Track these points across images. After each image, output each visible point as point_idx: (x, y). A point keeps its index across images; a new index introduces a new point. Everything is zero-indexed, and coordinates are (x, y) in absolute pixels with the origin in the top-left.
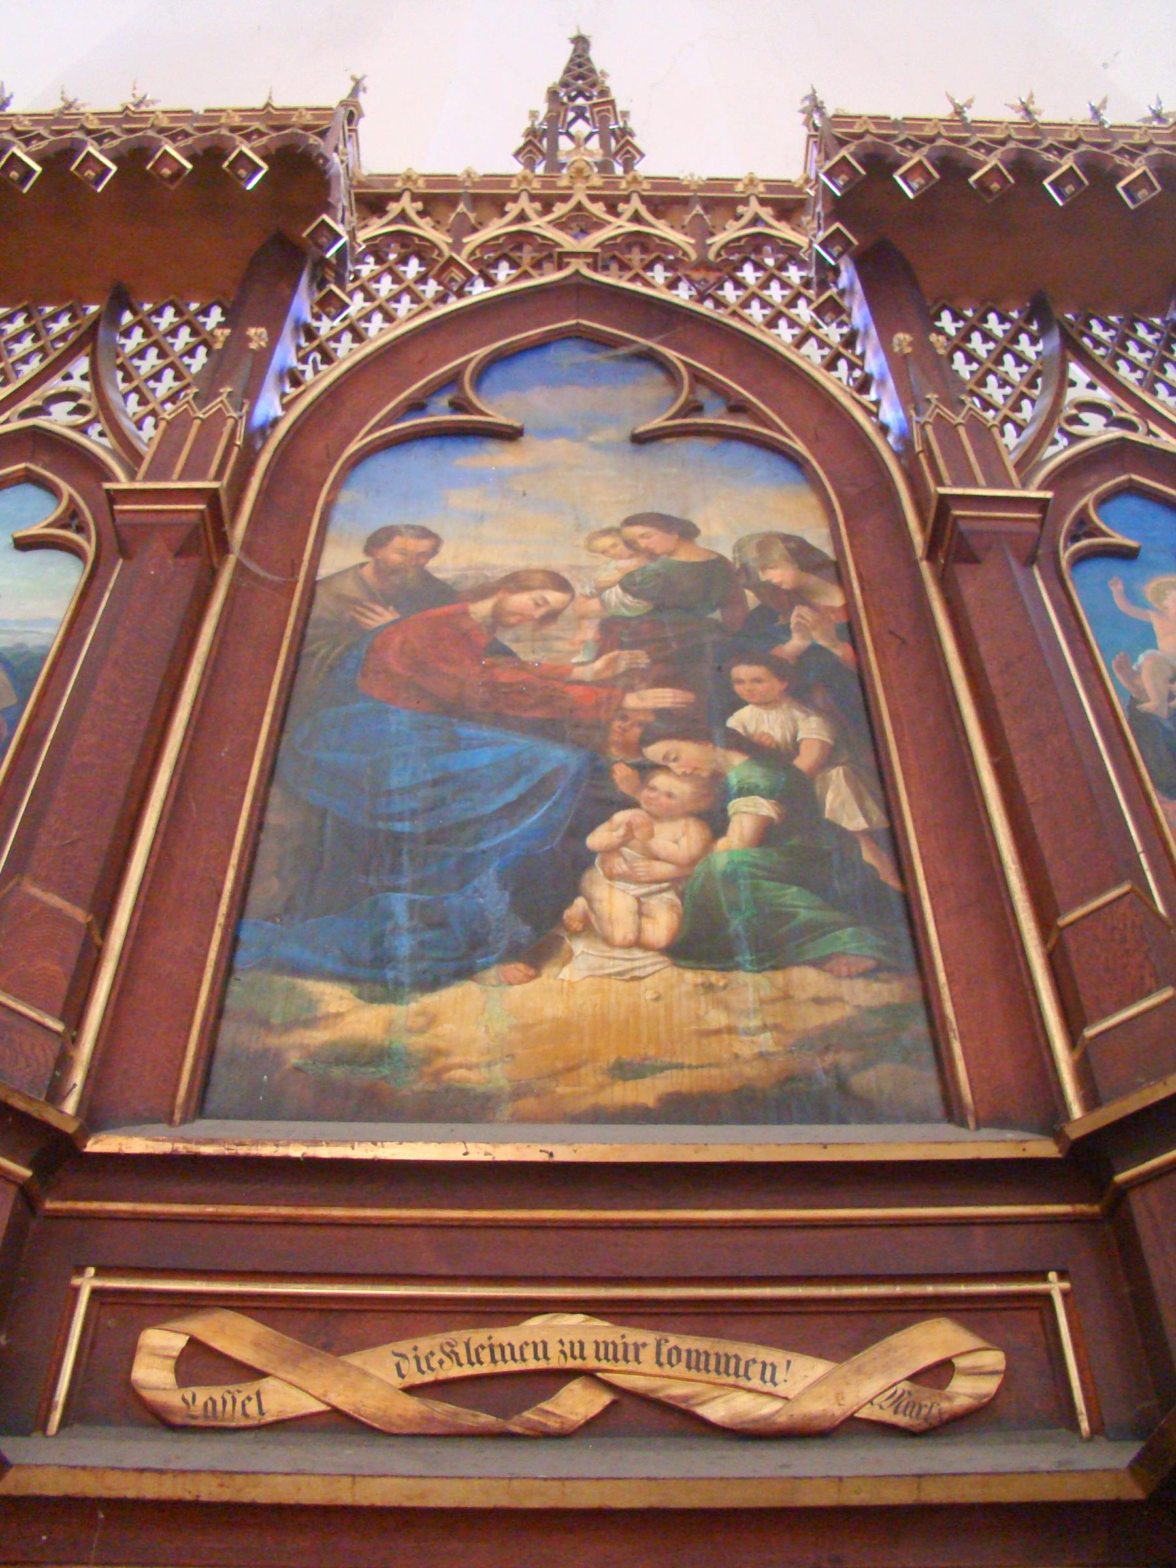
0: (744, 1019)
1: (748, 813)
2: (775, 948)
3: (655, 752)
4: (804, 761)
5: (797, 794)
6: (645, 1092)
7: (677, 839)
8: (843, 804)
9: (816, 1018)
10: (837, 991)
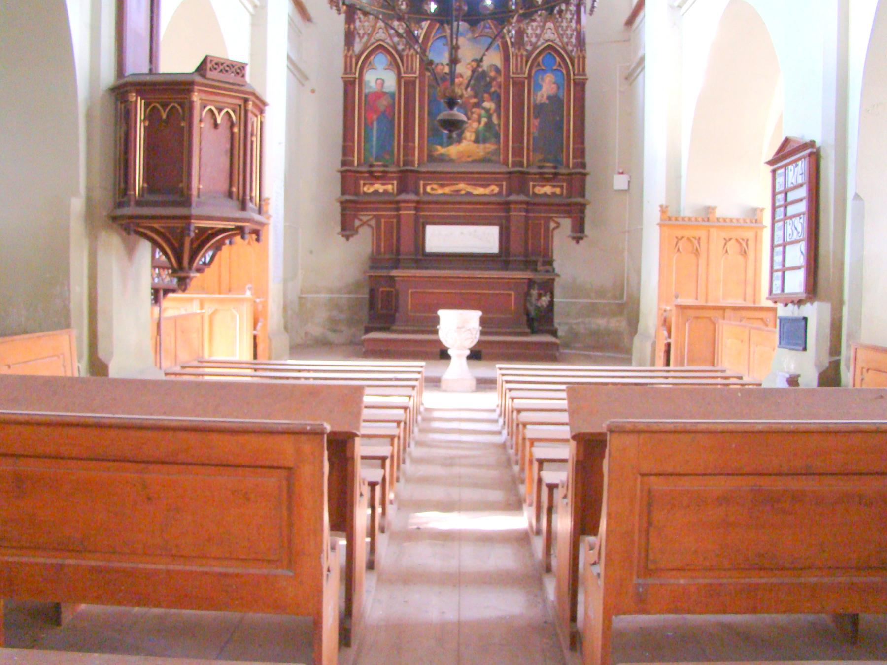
0: (481, 150)
1: (484, 120)
2: (485, 141)
3: (474, 110)
4: (491, 112)
5: (490, 117)
6: (470, 159)
7: (475, 125)
8: (495, 120)
9: (488, 150)
10: (490, 147)
